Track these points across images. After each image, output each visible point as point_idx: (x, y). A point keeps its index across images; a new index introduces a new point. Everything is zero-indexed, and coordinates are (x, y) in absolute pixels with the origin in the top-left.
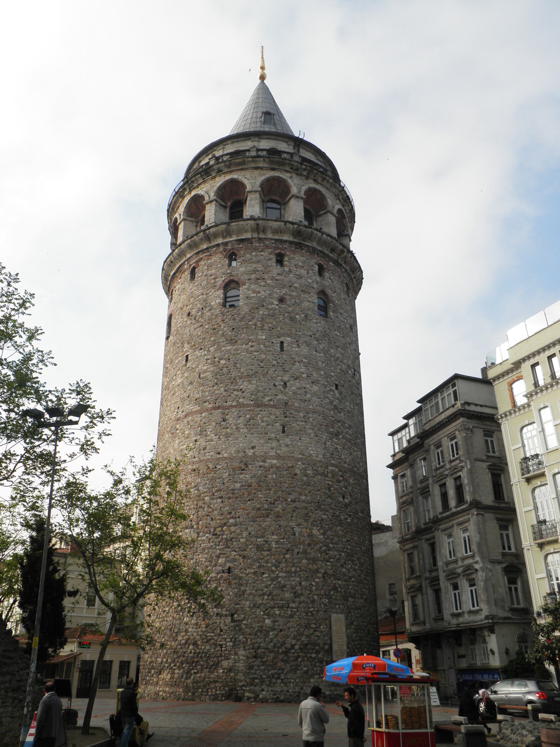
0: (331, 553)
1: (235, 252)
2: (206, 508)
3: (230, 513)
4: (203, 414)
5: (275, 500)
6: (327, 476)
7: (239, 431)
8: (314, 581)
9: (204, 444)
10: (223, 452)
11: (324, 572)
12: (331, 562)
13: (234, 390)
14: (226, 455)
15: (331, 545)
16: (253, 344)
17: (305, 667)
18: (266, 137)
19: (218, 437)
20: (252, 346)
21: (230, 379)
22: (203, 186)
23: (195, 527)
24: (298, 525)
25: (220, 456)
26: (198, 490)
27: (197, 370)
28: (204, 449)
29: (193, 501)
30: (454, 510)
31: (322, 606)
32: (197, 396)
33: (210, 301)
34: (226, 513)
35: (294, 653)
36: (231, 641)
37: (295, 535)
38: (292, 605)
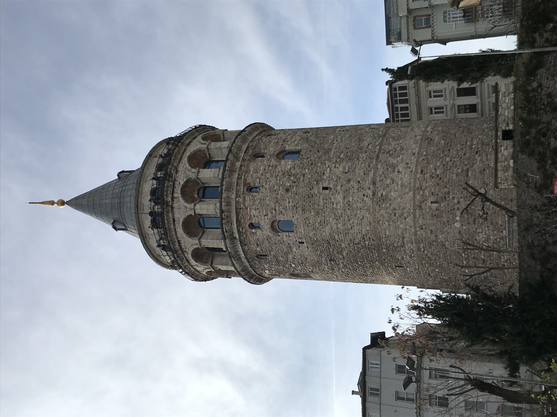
1: (253, 154)
4: (379, 167)
7: (400, 144)
9: (404, 165)
10: (414, 151)
13: (368, 148)
14: (417, 149)
16: (336, 140)
18: (158, 149)
19: (401, 155)
20: (337, 141)
21: (358, 151)
22: (177, 183)
23: (468, 166)
25: (417, 152)
26: (439, 167)
27: (340, 175)
28: (407, 164)
29: (447, 170)
30: (479, 100)
32: (362, 174)
33: (286, 170)
34: (461, 147)
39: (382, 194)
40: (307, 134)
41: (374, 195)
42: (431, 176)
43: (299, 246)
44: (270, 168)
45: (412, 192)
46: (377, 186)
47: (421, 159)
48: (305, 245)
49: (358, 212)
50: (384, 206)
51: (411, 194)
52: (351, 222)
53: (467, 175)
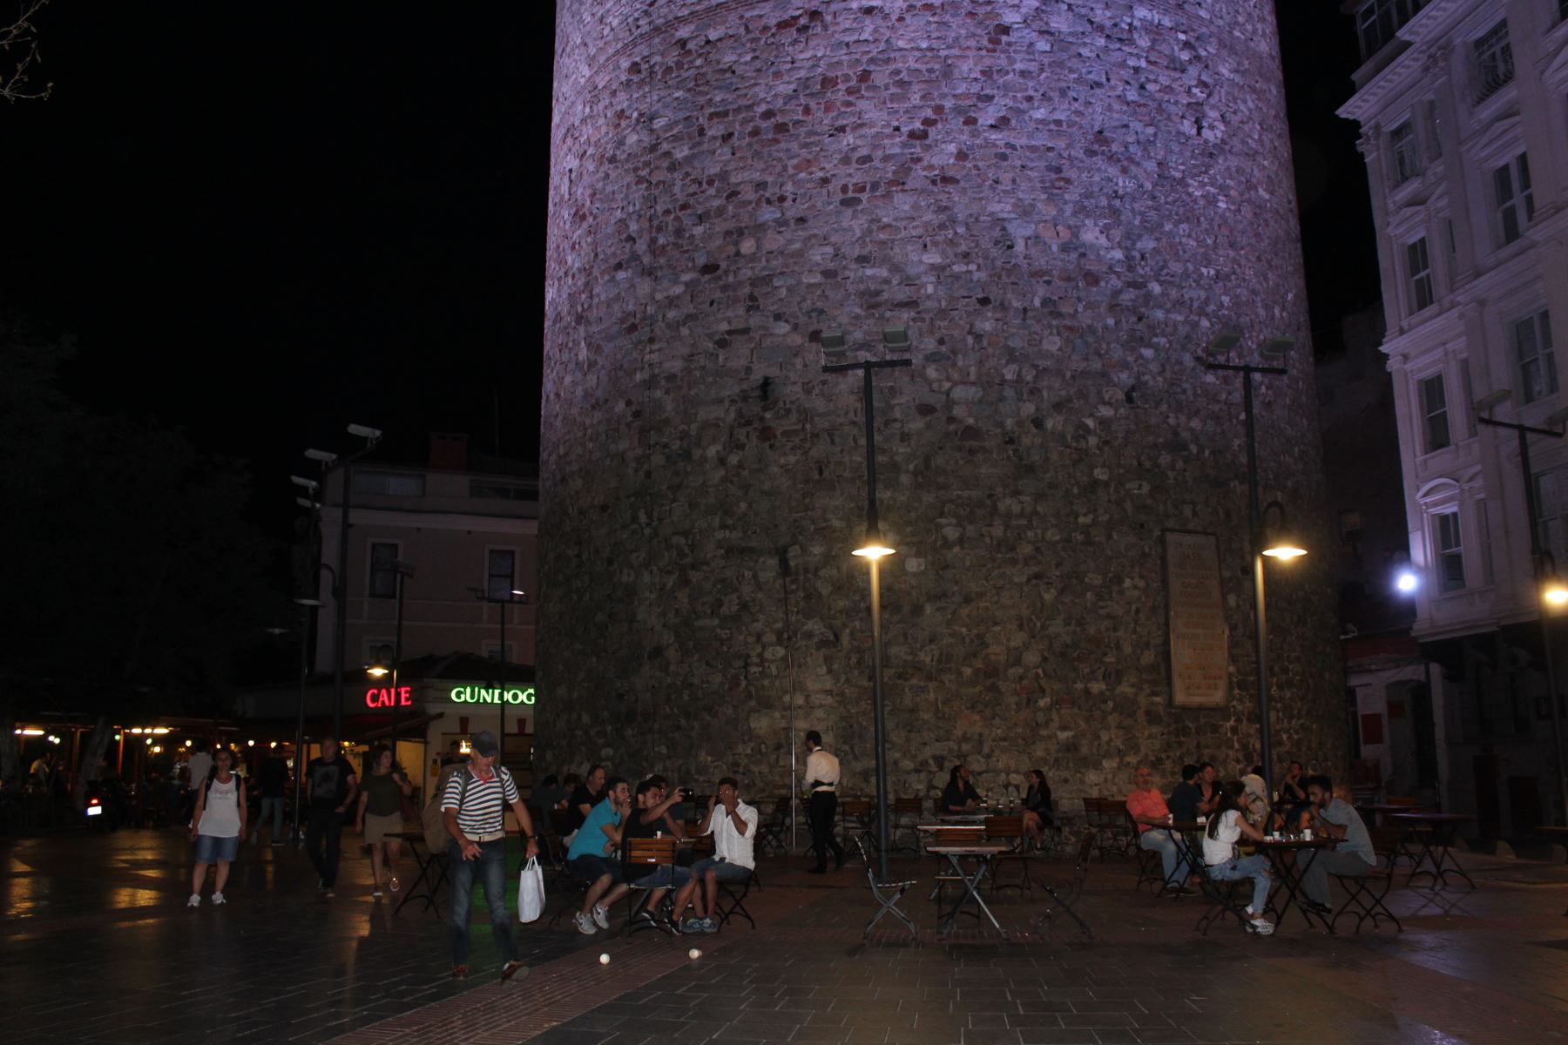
0: (1159, 315)
2: (679, 183)
3: (761, 186)
5: (928, 122)
6: (1131, 42)
8: (1092, 415)
11: (1132, 381)
12: (1155, 347)
15: (1156, 288)
17: (1064, 728)
24: (1026, 211)
31: (1128, 506)
35: (1021, 678)
36: (780, 642)
37: (1010, 247)
38: (1006, 504)
53: (619, 266)
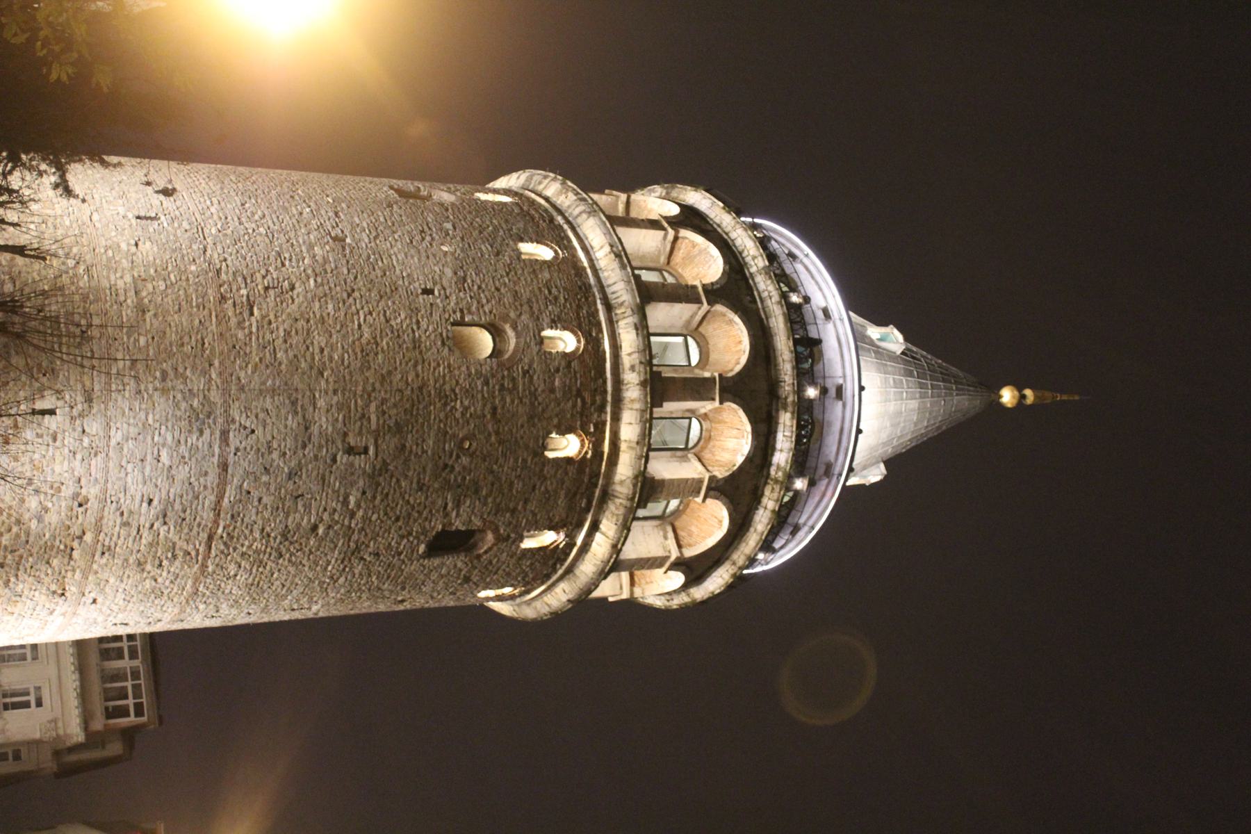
4: (207, 516)
14: (95, 566)
39: (201, 432)
40: (400, 598)
41: (225, 434)
42: (59, 490)
43: (435, 283)
44: (511, 506)
45: (113, 442)
46: (215, 460)
47: (88, 538)
48: (417, 287)
49: (269, 383)
50: (195, 403)
51: (116, 437)
52: (291, 354)
